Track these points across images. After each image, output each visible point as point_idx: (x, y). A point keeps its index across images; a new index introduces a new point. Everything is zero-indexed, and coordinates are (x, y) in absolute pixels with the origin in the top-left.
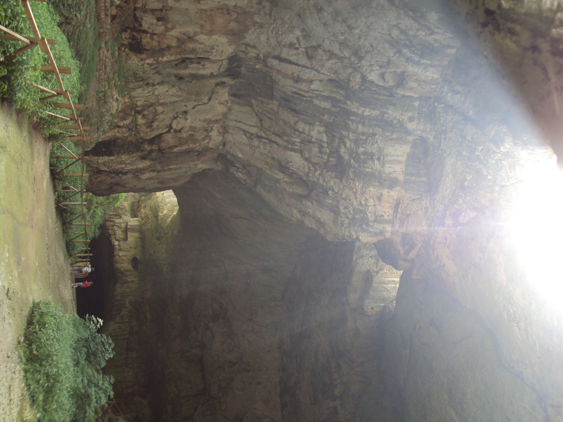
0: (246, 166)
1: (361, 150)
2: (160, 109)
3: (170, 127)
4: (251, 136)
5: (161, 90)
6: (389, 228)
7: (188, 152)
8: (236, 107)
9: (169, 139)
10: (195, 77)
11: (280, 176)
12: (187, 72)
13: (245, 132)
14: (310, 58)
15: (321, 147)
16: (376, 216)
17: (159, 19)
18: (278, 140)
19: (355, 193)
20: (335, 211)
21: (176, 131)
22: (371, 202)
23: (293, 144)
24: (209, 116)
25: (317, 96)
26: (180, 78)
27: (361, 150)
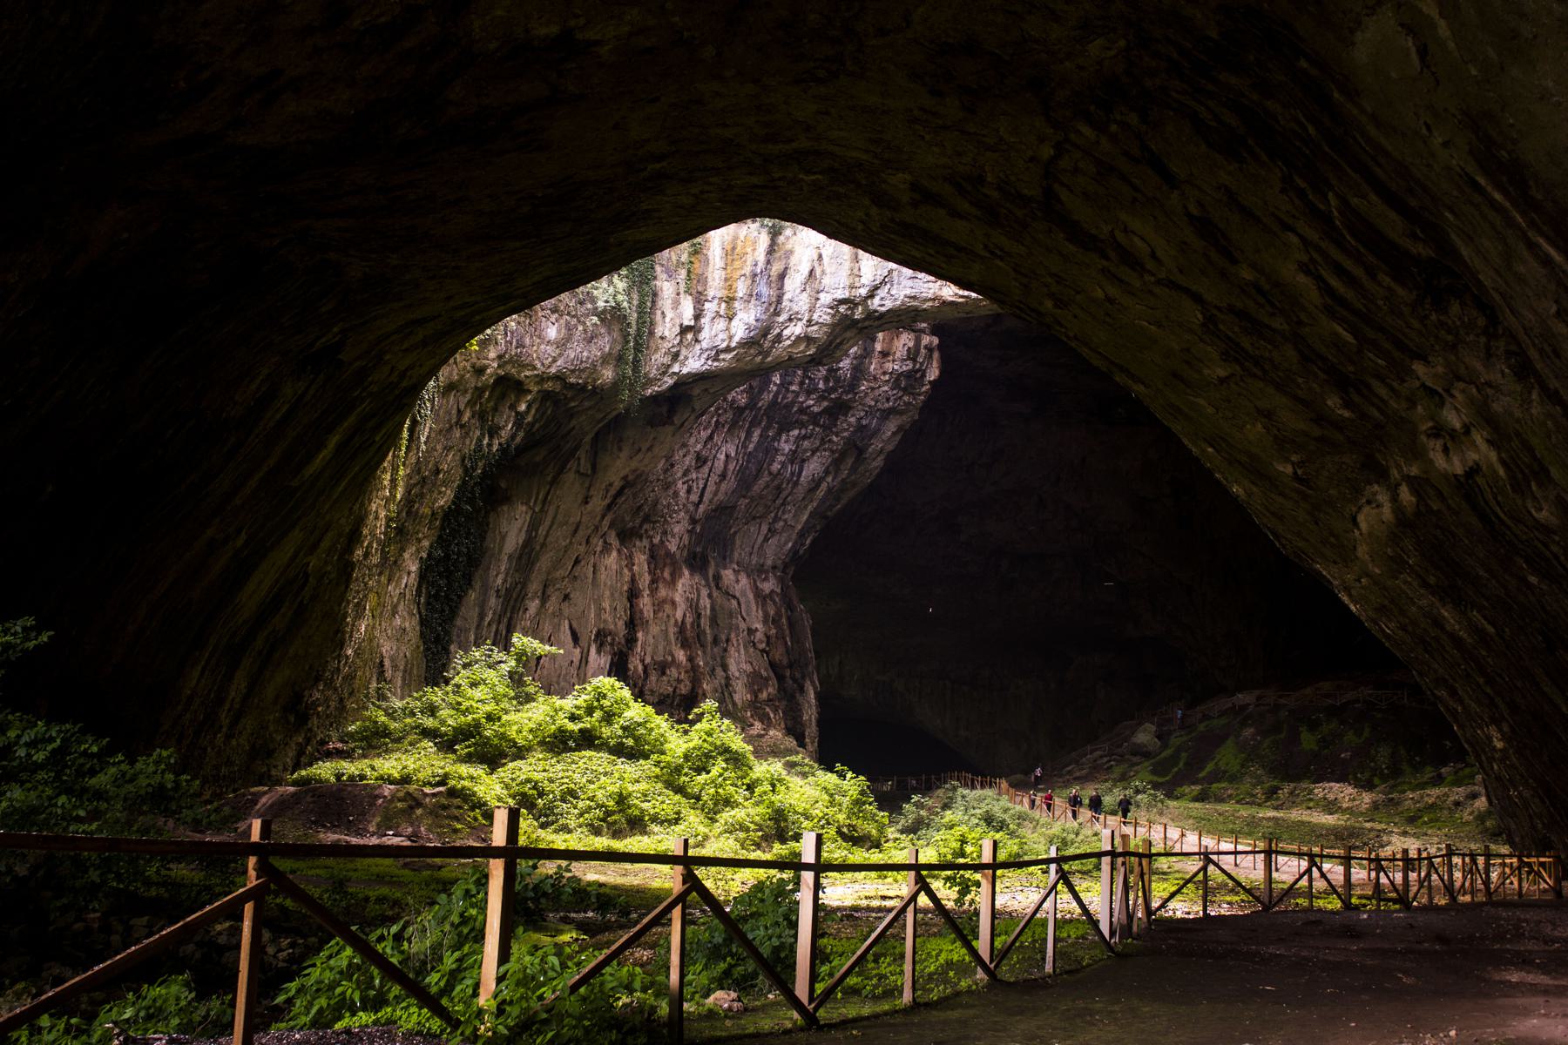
0: (802, 535)
1: (821, 385)
2: (749, 668)
3: (763, 651)
4: (772, 531)
5: (733, 668)
6: (926, 340)
7: (791, 625)
8: (736, 555)
9: (779, 654)
10: (714, 620)
11: (824, 486)
12: (708, 631)
13: (766, 539)
14: (705, 462)
15: (805, 437)
16: (909, 358)
17: (664, 673)
18: (783, 495)
19: (873, 389)
20: (887, 414)
21: (768, 644)
22: (889, 366)
23: (792, 474)
24: (751, 596)
25: (745, 446)
26: (716, 641)
27: (821, 385)
